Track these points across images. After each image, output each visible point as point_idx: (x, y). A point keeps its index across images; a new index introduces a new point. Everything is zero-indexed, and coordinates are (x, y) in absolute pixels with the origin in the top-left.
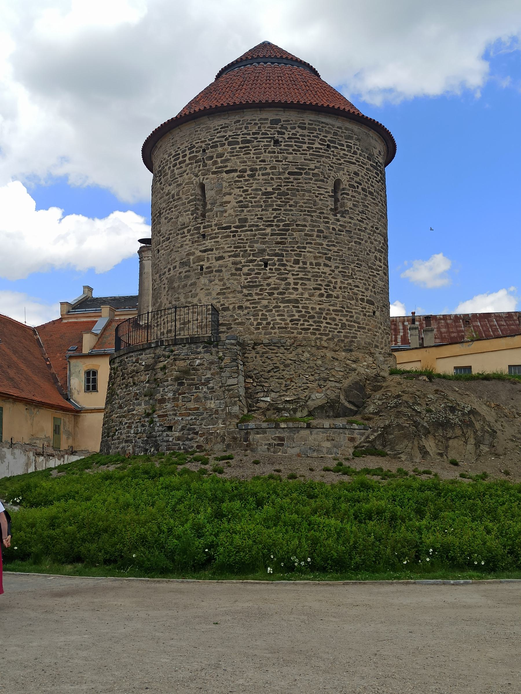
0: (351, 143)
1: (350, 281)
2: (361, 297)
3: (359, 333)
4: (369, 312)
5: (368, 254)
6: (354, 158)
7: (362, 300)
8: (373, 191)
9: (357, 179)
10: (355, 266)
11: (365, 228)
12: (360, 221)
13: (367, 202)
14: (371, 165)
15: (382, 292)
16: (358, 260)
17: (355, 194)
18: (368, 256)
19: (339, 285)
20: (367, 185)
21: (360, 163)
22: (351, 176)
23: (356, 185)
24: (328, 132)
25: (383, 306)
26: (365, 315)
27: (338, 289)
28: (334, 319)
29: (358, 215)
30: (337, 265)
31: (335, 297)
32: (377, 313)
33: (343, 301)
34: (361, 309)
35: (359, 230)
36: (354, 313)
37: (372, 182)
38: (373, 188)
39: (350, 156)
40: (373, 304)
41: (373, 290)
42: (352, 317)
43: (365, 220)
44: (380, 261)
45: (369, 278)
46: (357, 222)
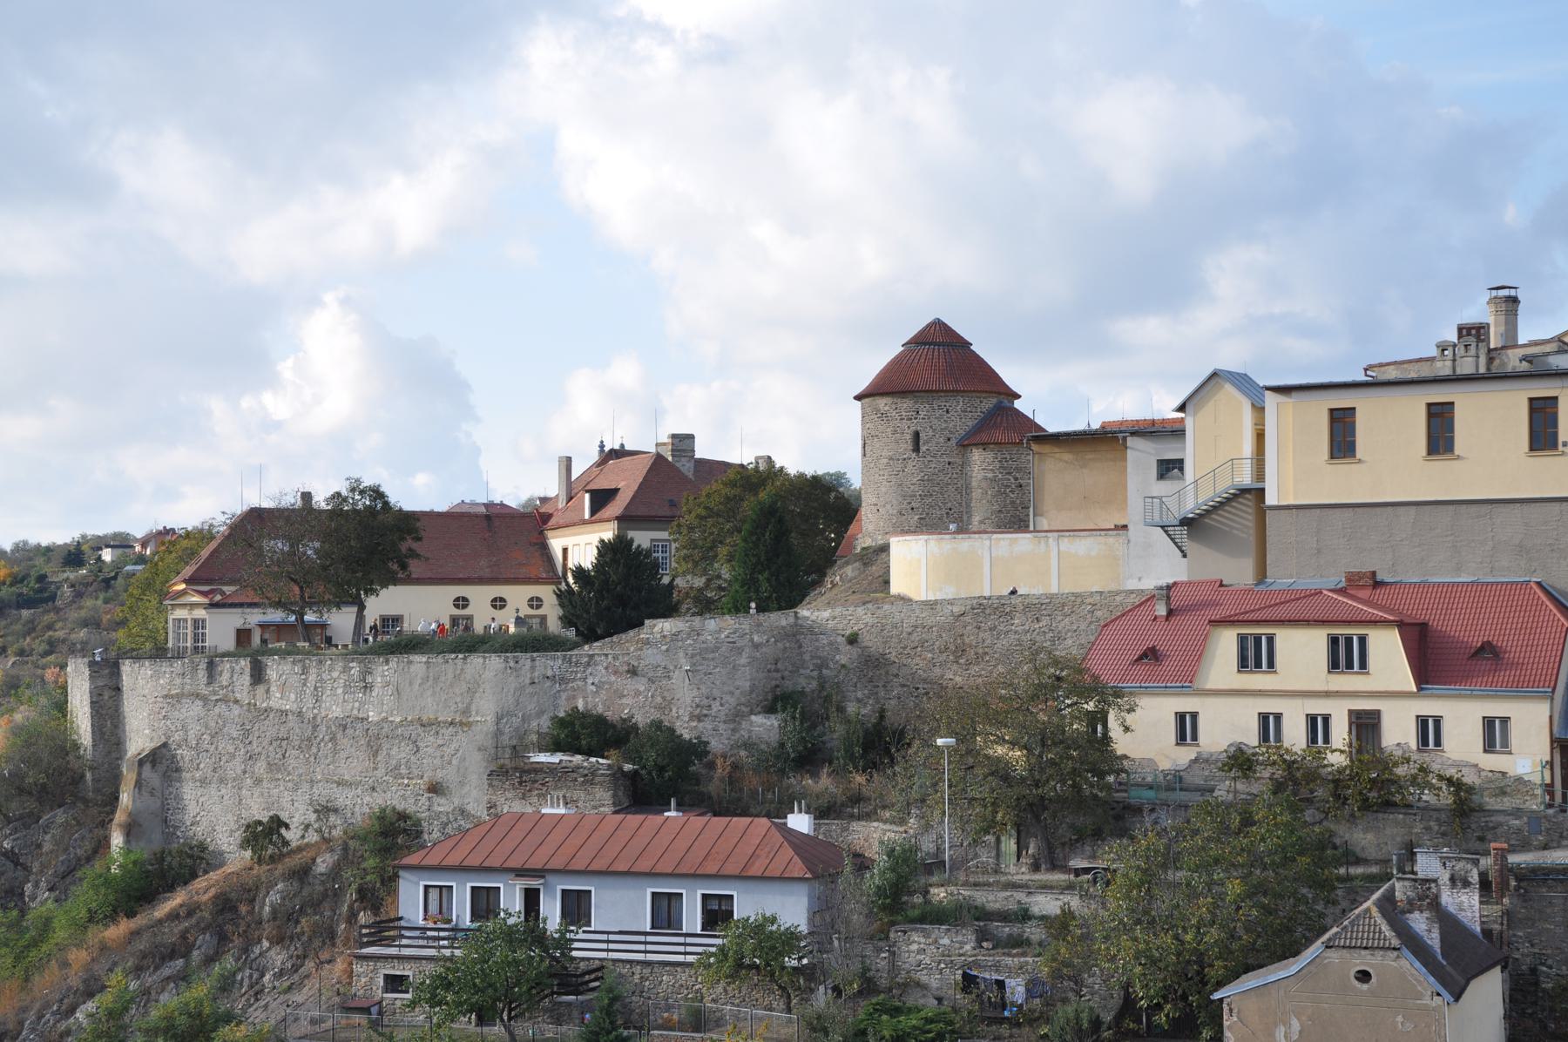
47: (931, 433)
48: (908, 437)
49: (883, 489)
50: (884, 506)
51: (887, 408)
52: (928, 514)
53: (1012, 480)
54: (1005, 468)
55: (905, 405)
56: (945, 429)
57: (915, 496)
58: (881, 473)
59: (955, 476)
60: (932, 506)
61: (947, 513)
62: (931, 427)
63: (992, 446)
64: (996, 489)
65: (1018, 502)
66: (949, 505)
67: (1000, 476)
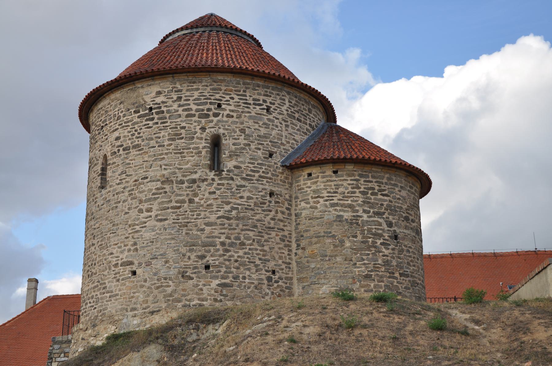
0: (116, 111)
1: (105, 252)
2: (113, 263)
3: (109, 303)
4: (124, 275)
5: (126, 213)
6: (117, 124)
7: (116, 265)
8: (140, 142)
9: (119, 143)
10: (111, 234)
11: (124, 188)
12: (119, 184)
13: (130, 158)
14: (139, 117)
15: (150, 244)
16: (114, 225)
17: (115, 160)
18: (126, 216)
19: (98, 259)
20: (130, 142)
21: (124, 125)
22: (113, 144)
23: (116, 150)
24: (102, 115)
25: (151, 259)
26: (118, 280)
27: (97, 264)
28: (92, 297)
29: (117, 178)
30: (98, 240)
31: (95, 274)
32: (138, 272)
33: (99, 275)
34: (114, 276)
35: (117, 194)
36: (107, 283)
37: (139, 133)
38: (140, 139)
39: (114, 124)
40: (131, 263)
41: (132, 248)
42: (104, 288)
43: (124, 179)
44: (149, 210)
45: (127, 238)
46: (116, 186)
47: (242, 140)
48: (203, 145)
49: (148, 235)
50: (148, 264)
51: (159, 100)
52: (236, 278)
53: (385, 226)
54: (372, 205)
55: (196, 94)
56: (265, 137)
57: (213, 245)
58: (145, 206)
59: (280, 216)
60: (243, 264)
61: (269, 279)
62: (243, 131)
63: (350, 167)
64: (360, 238)
65: (394, 263)
66: (271, 265)
67: (365, 217)
